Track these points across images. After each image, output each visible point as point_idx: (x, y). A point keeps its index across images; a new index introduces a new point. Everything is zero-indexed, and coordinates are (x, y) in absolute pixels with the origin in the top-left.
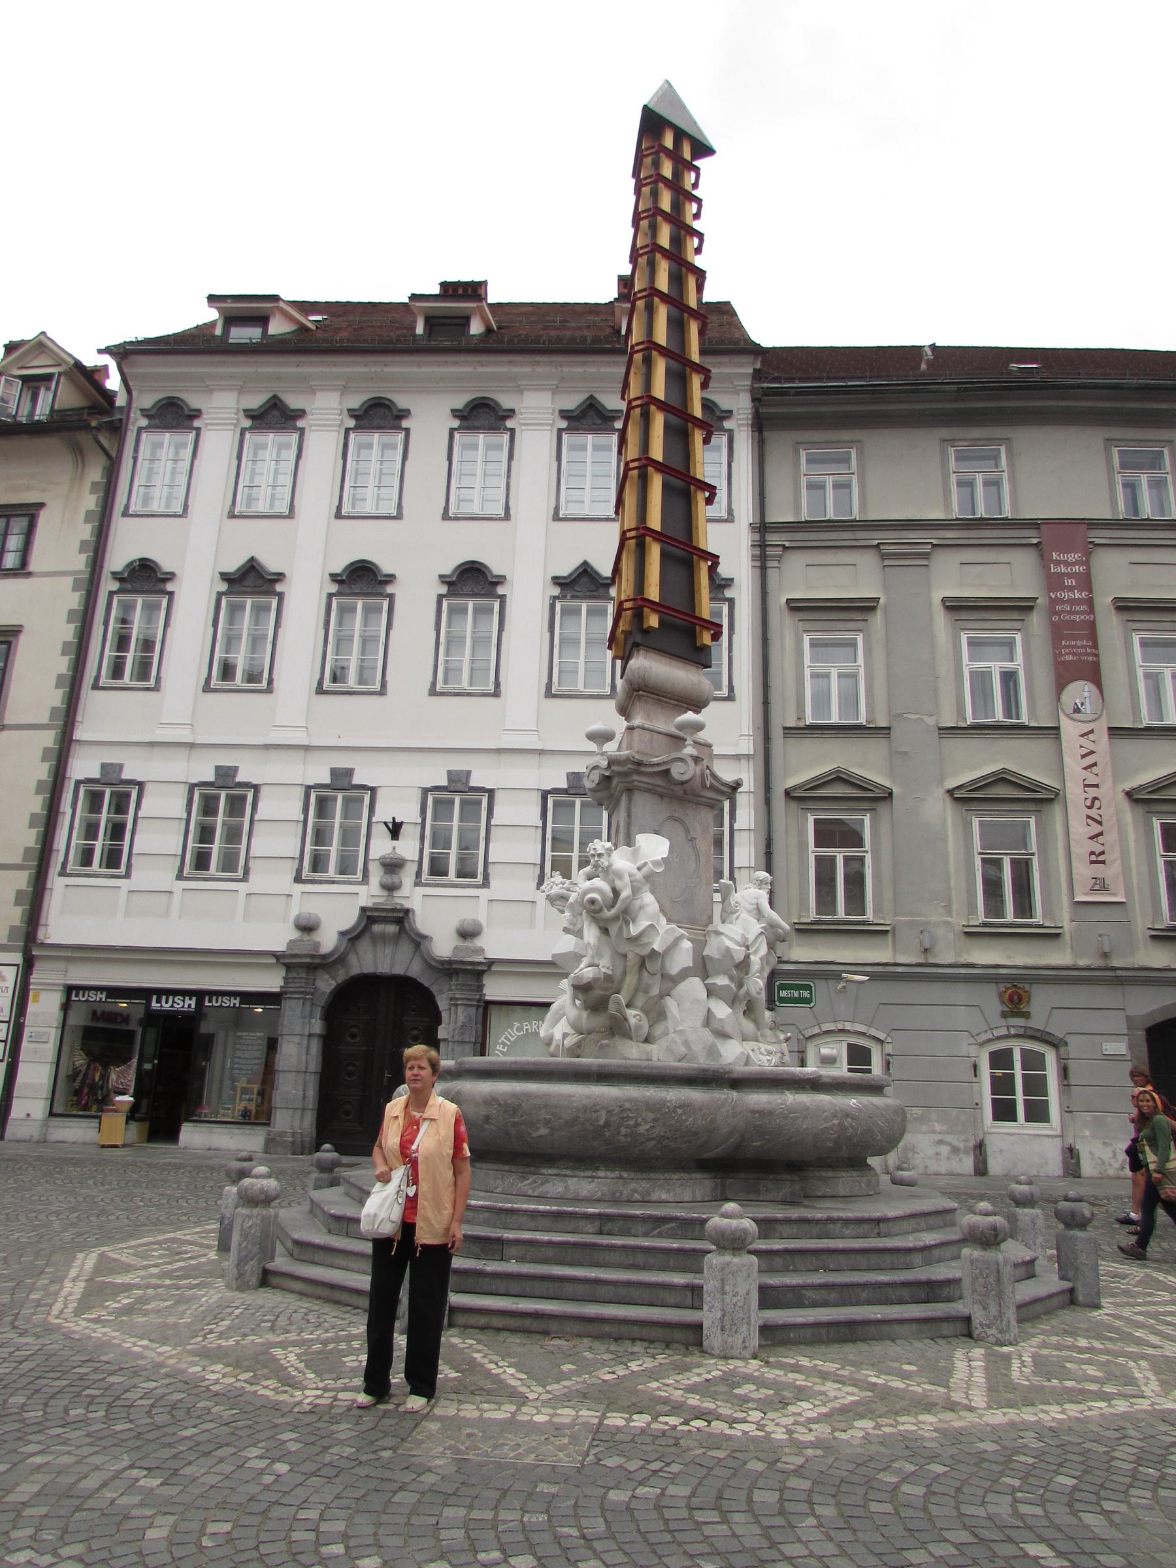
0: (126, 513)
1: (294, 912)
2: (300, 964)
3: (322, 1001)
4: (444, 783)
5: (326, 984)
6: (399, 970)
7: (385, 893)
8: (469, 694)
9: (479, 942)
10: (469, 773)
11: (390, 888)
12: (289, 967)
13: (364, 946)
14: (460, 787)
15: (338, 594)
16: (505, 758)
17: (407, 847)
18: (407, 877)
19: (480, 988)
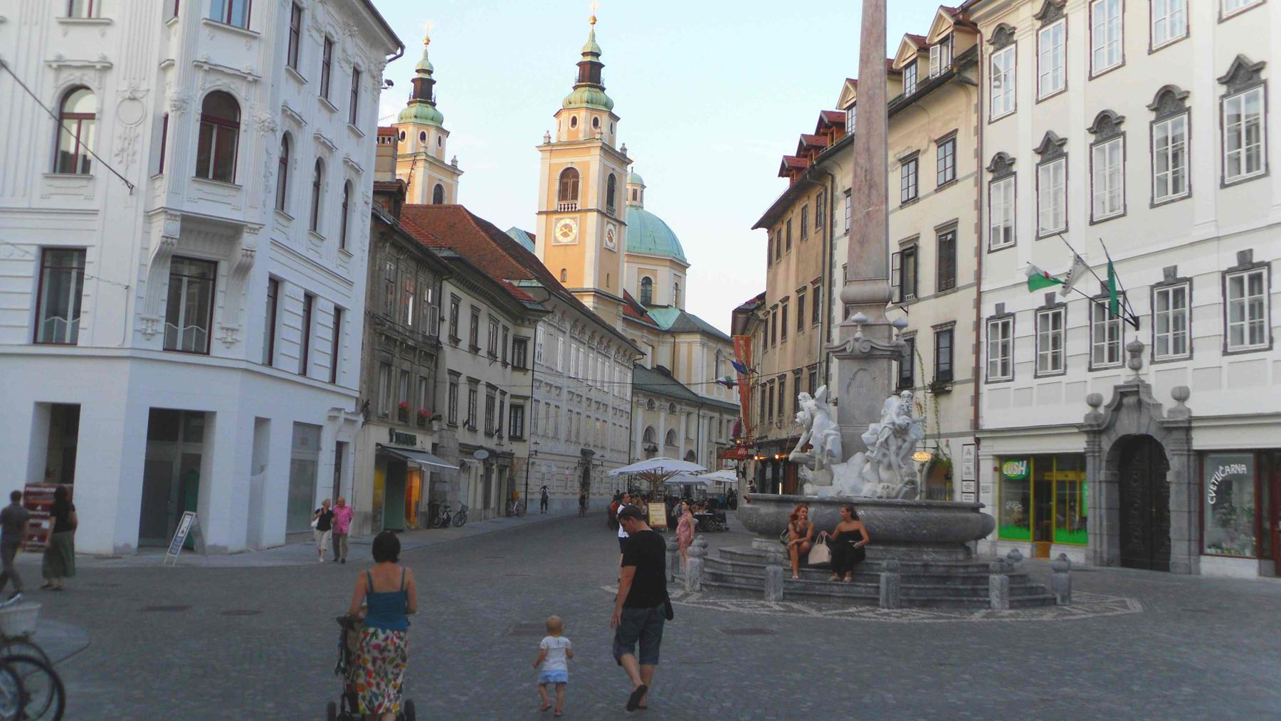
0: (990, 123)
1: (1089, 392)
2: (1094, 430)
3: (1105, 457)
4: (1162, 279)
5: (1107, 443)
6: (1143, 431)
7: (1134, 373)
8: (1173, 201)
9: (1188, 404)
10: (1175, 267)
11: (1136, 368)
12: (1087, 432)
13: (1124, 412)
14: (1171, 280)
15: (1096, 143)
16: (1197, 248)
17: (1144, 335)
18: (1145, 357)
19: (1189, 440)
